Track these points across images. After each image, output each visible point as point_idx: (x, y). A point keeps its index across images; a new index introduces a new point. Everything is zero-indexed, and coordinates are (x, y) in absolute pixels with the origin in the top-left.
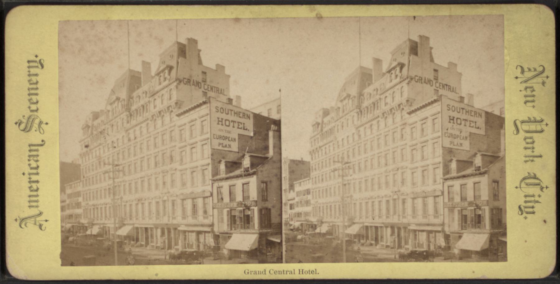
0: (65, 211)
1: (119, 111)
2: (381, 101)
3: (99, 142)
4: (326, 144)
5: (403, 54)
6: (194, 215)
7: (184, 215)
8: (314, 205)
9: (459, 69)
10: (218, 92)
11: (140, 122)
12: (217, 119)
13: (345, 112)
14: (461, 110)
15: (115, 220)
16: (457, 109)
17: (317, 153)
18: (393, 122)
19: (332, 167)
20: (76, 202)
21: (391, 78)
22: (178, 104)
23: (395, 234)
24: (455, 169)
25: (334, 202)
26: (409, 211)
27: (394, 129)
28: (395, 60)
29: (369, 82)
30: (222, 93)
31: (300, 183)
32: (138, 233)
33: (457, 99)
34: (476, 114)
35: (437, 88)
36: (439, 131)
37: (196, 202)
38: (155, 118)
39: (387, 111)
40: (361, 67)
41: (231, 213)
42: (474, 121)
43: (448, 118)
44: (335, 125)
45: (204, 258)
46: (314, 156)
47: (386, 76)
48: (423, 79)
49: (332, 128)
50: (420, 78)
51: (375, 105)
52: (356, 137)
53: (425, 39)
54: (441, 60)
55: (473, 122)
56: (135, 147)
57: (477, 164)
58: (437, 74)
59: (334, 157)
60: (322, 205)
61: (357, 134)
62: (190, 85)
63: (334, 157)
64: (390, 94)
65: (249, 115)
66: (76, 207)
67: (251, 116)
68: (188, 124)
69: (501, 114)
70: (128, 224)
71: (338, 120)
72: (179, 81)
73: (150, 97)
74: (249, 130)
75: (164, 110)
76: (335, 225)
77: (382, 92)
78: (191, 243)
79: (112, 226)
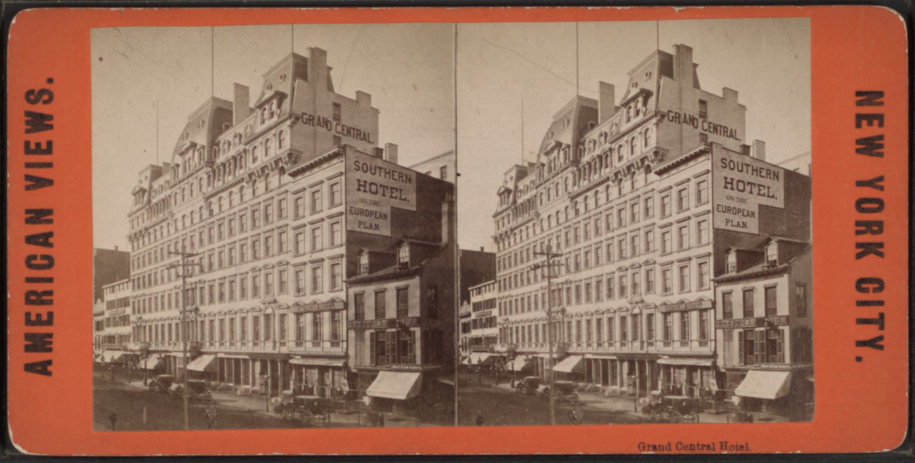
0: (102, 329)
1: (195, 167)
2: (611, 152)
3: (161, 215)
4: (522, 225)
5: (283, 77)
6: (317, 339)
7: (300, 339)
8: (502, 324)
9: (741, 101)
10: (359, 137)
11: (229, 184)
12: (357, 182)
13: (553, 172)
14: (378, 170)
15: (185, 345)
16: (371, 169)
17: (506, 239)
18: (633, 187)
19: (532, 262)
20: (121, 315)
21: (629, 115)
22: (293, 156)
23: (635, 372)
24: (735, 264)
25: (522, 321)
26: (291, 334)
27: (635, 198)
28: (270, 87)
29: (592, 122)
30: (365, 139)
31: (480, 288)
32: (222, 368)
33: (738, 149)
34: (770, 174)
35: (706, 130)
36: (341, 204)
37: (320, 318)
38: (254, 178)
39: (255, 171)
40: (215, 99)
41: (377, 338)
42: (399, 188)
43: (724, 180)
44: (172, 193)
45: (329, 412)
46: (135, 244)
47: (620, 113)
48: (682, 117)
49: (166, 198)
50: (311, 118)
51: (236, 160)
52: (206, 213)
53: (685, 50)
54: (711, 84)
55: (396, 189)
56: (220, 226)
57: (403, 258)
58: (706, 108)
59: (535, 247)
60: (154, 323)
61: (573, 208)
62: (313, 125)
63: (535, 247)
64: (627, 142)
65: (410, 175)
66: (122, 323)
67: (414, 177)
68: (309, 190)
69: (442, 177)
70: (206, 353)
71: (175, 185)
72: (296, 119)
73: (246, 144)
74: (408, 201)
75: (269, 165)
76: (536, 358)
77: (249, 140)
78: (310, 386)
79: (181, 355)
